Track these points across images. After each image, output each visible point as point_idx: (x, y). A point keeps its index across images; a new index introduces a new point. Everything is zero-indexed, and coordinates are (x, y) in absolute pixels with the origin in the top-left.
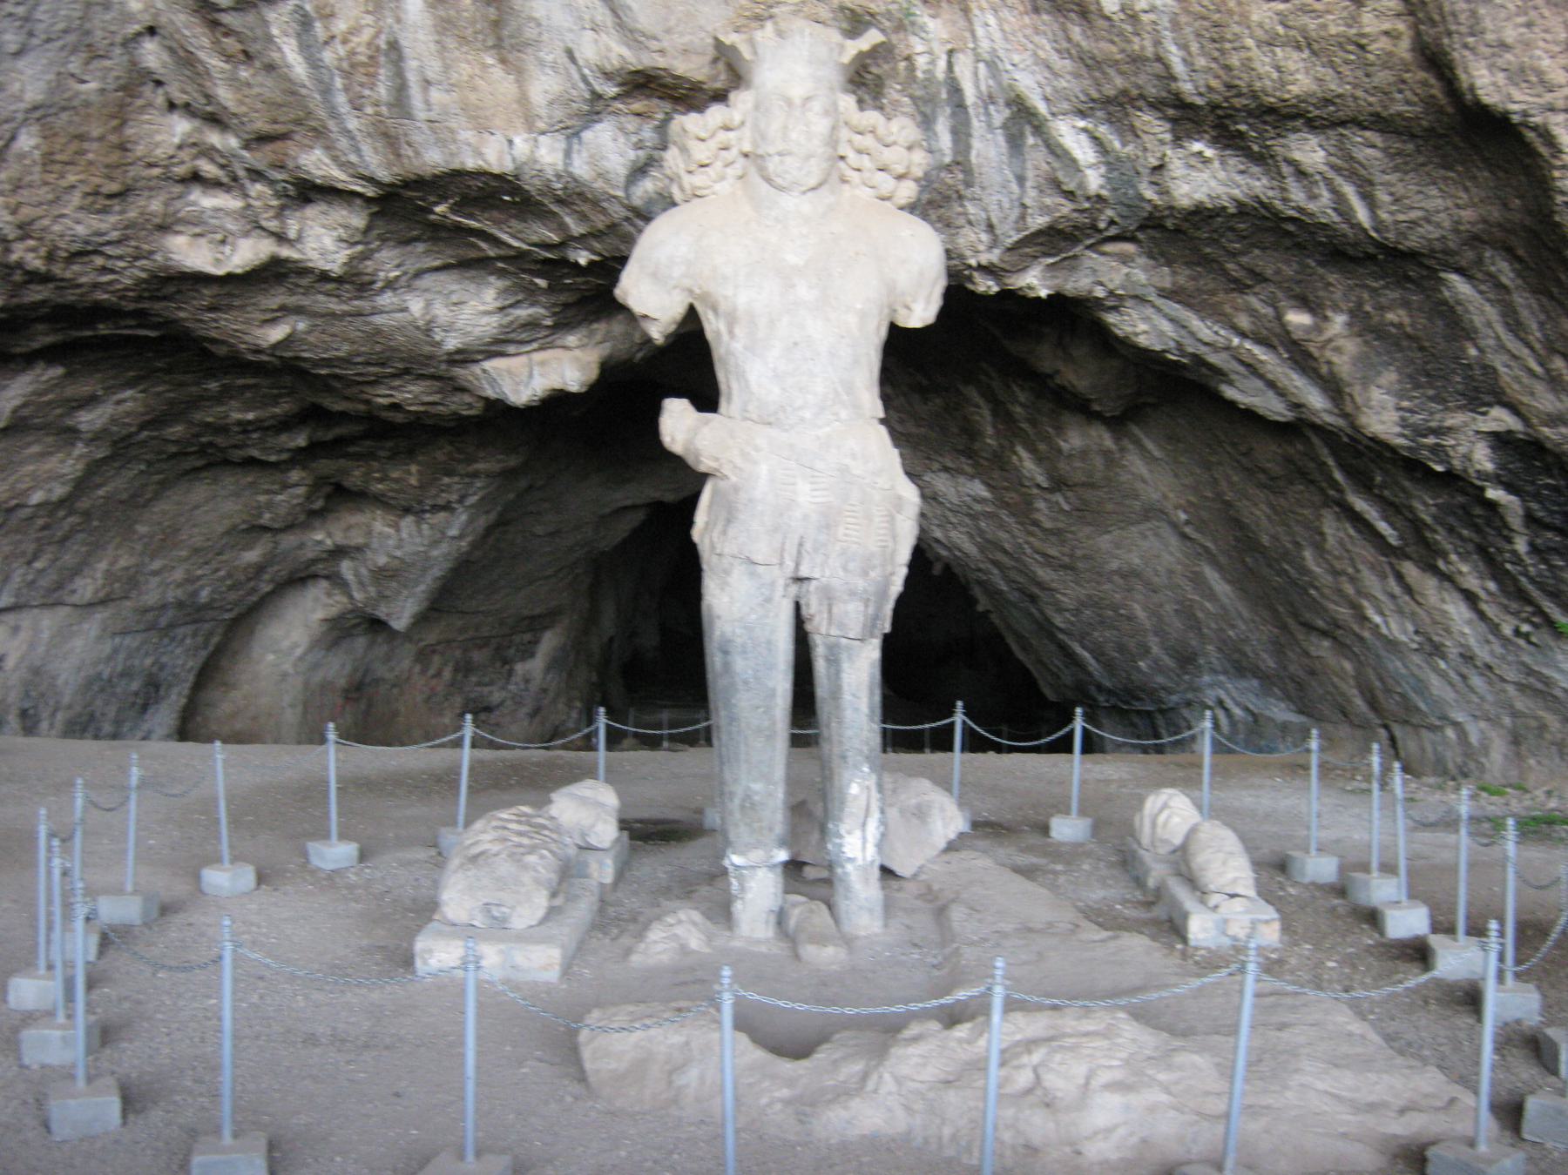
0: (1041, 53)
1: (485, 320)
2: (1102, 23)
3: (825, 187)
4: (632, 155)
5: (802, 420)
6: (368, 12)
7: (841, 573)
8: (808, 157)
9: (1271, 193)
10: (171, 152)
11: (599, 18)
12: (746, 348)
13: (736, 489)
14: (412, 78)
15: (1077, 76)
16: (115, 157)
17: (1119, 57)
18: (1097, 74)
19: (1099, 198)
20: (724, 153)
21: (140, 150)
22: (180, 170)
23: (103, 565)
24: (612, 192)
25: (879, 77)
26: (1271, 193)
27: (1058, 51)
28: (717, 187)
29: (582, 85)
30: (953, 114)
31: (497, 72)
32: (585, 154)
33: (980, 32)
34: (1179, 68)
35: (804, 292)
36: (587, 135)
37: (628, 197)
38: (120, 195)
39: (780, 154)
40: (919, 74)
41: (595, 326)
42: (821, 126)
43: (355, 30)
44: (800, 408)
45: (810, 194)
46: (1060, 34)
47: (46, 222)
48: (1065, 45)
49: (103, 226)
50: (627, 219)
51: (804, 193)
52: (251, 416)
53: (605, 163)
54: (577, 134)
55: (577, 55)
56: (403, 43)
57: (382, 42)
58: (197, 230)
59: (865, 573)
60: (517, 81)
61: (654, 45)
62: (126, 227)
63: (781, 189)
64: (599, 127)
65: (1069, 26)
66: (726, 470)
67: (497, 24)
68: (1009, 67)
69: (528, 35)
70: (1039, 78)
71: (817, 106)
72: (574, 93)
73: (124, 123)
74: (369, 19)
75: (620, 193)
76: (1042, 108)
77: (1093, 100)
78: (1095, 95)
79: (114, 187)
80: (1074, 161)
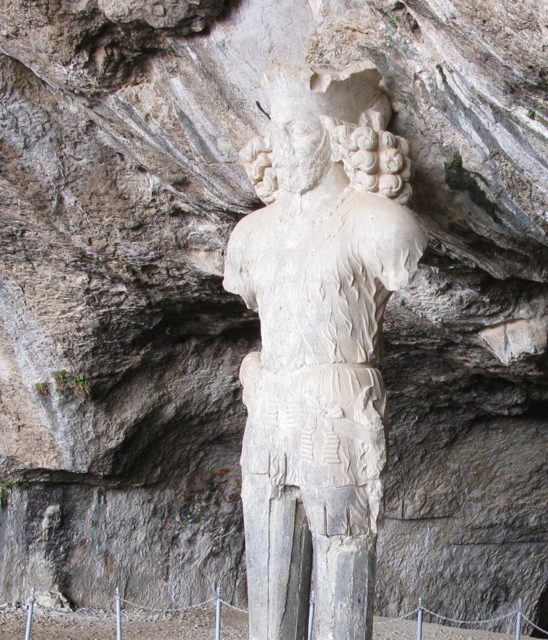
1: (439, 300)
3: (320, 187)
6: (158, 95)
8: (295, 167)
10: (151, 198)
14: (203, 135)
16: (120, 204)
20: (267, 170)
21: (134, 198)
22: (165, 208)
23: (420, 491)
25: (410, 94)
28: (275, 194)
30: (465, 114)
31: (239, 123)
35: (290, 269)
38: (140, 226)
40: (429, 89)
41: (535, 301)
42: (302, 142)
43: (157, 109)
44: (280, 356)
45: (308, 193)
47: (111, 249)
49: (144, 249)
51: (303, 192)
52: (442, 379)
56: (187, 113)
57: (174, 112)
58: (207, 247)
59: (318, 483)
60: (253, 129)
62: (155, 249)
67: (221, 92)
71: (296, 128)
73: (114, 182)
74: (161, 100)
79: (131, 223)
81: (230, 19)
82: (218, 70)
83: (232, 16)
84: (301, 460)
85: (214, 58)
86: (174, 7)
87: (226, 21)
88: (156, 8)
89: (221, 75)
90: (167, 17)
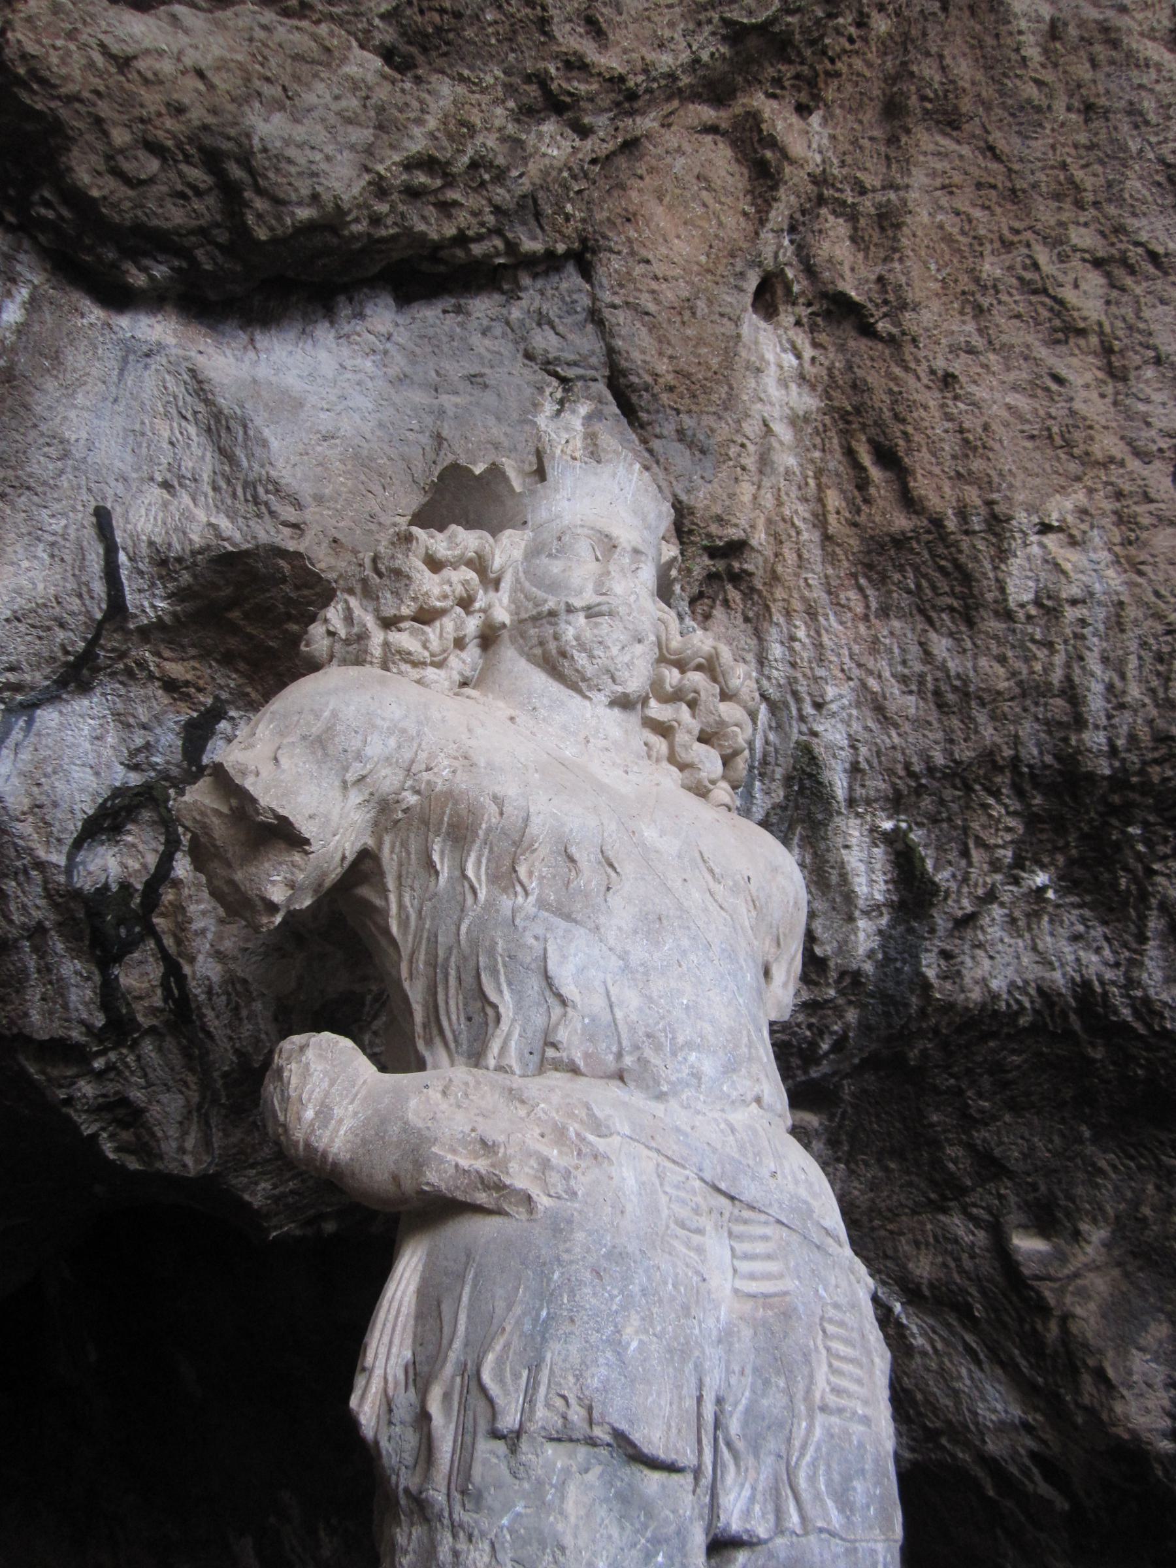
0: (872, 683)
2: (994, 625)
4: (120, 776)
5: (697, 1075)
7: (836, 1519)
9: (1109, 975)
11: (188, 464)
12: (542, 904)
13: (559, 1227)
15: (921, 724)
17: (1003, 685)
18: (956, 723)
19: (857, 974)
24: (42, 853)
26: (1109, 975)
27: (904, 680)
29: (99, 588)
32: (25, 755)
33: (777, 651)
34: (1096, 704)
36: (48, 717)
37: (69, 870)
39: (591, 612)
44: (689, 1045)
46: (914, 650)
48: (918, 667)
50: (38, 931)
53: (60, 786)
54: (30, 707)
55: (117, 522)
61: (288, 513)
63: (575, 683)
64: (82, 704)
65: (933, 636)
66: (520, 1178)
68: (809, 710)
69: (35, 469)
70: (856, 726)
72: (75, 604)
75: (58, 858)
76: (839, 783)
77: (931, 770)
78: (939, 759)
80: (849, 897)
81: (210, 327)
82: (50, 385)
83: (221, 327)
84: (820, 1418)
85: (75, 358)
86: (182, 195)
87: (201, 323)
88: (142, 154)
89: (41, 403)
90: (130, 193)
